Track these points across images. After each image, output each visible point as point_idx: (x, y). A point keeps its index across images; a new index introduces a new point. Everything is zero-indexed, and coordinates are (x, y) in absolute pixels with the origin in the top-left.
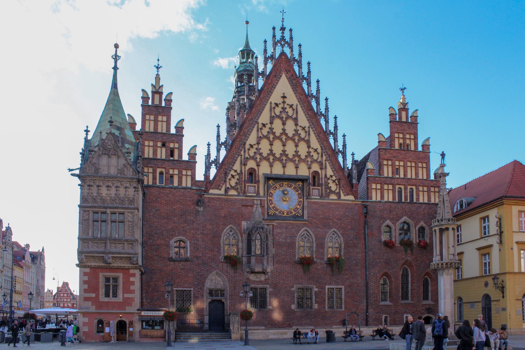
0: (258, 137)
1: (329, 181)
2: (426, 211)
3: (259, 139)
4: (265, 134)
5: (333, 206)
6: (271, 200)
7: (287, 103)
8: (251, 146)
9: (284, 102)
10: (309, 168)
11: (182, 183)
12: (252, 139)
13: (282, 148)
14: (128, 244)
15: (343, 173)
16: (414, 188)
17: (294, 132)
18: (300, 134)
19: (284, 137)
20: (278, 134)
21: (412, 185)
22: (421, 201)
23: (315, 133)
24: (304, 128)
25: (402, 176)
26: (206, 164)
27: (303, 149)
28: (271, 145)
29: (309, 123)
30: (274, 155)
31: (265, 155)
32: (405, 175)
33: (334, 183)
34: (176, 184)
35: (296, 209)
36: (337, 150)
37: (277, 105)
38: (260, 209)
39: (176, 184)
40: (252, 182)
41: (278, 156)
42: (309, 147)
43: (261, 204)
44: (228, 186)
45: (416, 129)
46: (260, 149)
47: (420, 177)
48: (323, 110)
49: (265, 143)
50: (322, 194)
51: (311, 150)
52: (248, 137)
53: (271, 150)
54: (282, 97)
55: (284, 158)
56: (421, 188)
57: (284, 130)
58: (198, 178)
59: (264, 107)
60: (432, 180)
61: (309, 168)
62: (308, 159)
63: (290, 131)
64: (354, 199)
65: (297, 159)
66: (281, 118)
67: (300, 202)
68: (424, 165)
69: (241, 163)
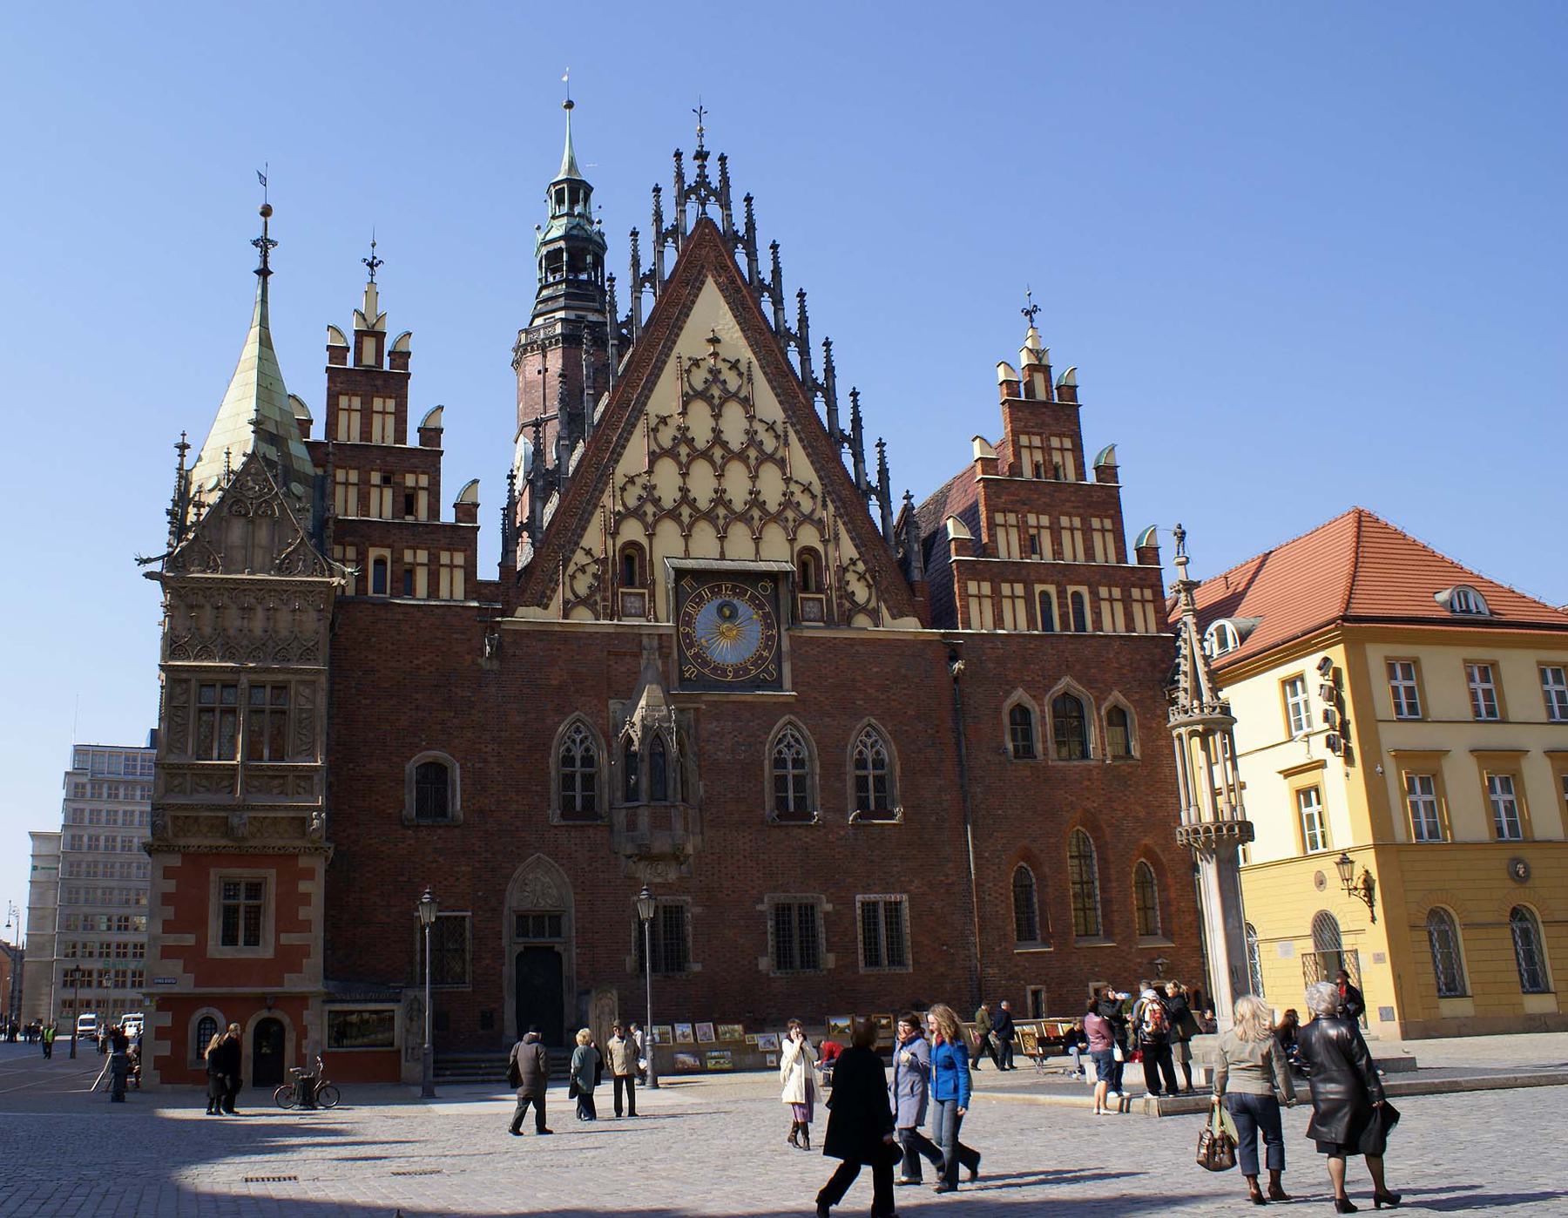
1: (850, 576)
3: (654, 458)
4: (667, 442)
5: (862, 649)
6: (688, 635)
7: (722, 355)
8: (631, 481)
9: (715, 355)
11: (438, 590)
14: (298, 777)
15: (886, 551)
18: (761, 443)
19: (718, 453)
20: (701, 444)
21: (1080, 583)
23: (801, 440)
24: (771, 427)
25: (1048, 557)
26: (504, 532)
27: (771, 486)
28: (684, 475)
29: (785, 410)
30: (692, 503)
31: (668, 503)
32: (1058, 553)
33: (863, 583)
35: (758, 660)
36: (864, 487)
37: (696, 363)
38: (659, 663)
40: (631, 584)
41: (703, 504)
43: (661, 647)
46: (654, 487)
47: (1100, 559)
48: (819, 375)
49: (667, 468)
51: (794, 488)
52: (620, 455)
53: (684, 490)
55: (721, 512)
56: (1104, 592)
57: (717, 432)
58: (482, 575)
59: (661, 369)
60: (1133, 568)
61: (792, 541)
62: (787, 515)
63: (735, 438)
65: (756, 513)
66: (709, 399)
67: (769, 638)
68: (1108, 524)
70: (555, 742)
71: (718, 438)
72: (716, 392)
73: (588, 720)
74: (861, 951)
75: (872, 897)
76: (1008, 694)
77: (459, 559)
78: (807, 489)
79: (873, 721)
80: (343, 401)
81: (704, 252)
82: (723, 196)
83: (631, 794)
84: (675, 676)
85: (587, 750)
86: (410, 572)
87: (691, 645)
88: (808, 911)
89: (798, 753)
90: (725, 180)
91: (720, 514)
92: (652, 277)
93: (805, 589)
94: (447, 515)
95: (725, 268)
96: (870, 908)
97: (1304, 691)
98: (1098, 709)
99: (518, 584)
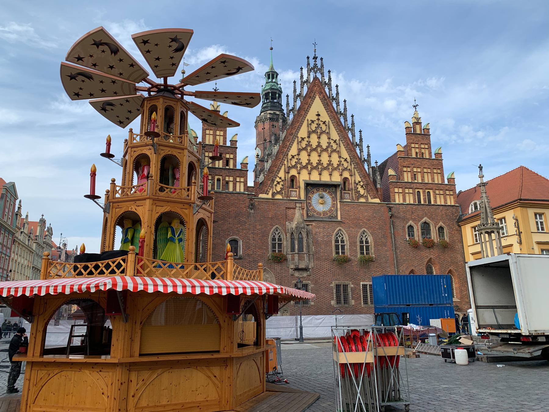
0: (298, 149)
1: (359, 187)
2: (443, 213)
3: (300, 150)
5: (362, 208)
7: (321, 119)
8: (293, 157)
9: (318, 119)
10: (341, 175)
12: (293, 151)
13: (318, 158)
16: (431, 191)
17: (327, 145)
22: (439, 203)
23: (344, 145)
24: (335, 142)
27: (335, 159)
28: (309, 155)
32: (422, 180)
34: (231, 189)
35: (330, 210)
37: (313, 122)
39: (231, 189)
40: (293, 187)
42: (340, 157)
44: (274, 191)
45: (429, 139)
49: (304, 154)
50: (352, 197)
53: (309, 160)
54: (317, 115)
57: (319, 143)
59: (302, 124)
61: (341, 175)
63: (324, 145)
64: (379, 202)
69: (285, 171)
70: (270, 234)
71: (319, 145)
72: (319, 131)
73: (280, 228)
74: (362, 300)
75: (365, 283)
76: (407, 223)
77: (242, 180)
78: (346, 160)
79: (365, 229)
80: (207, 132)
81: (315, 88)
82: (321, 70)
83: (293, 249)
84: (305, 215)
85: (280, 236)
86: (227, 183)
87: (310, 206)
88: (346, 286)
89: (342, 238)
90: (322, 66)
91: (319, 167)
92: (300, 95)
93: (345, 190)
94: (239, 167)
95: (322, 93)
96: (365, 286)
97: (505, 223)
98: (435, 227)
99: (260, 187)
